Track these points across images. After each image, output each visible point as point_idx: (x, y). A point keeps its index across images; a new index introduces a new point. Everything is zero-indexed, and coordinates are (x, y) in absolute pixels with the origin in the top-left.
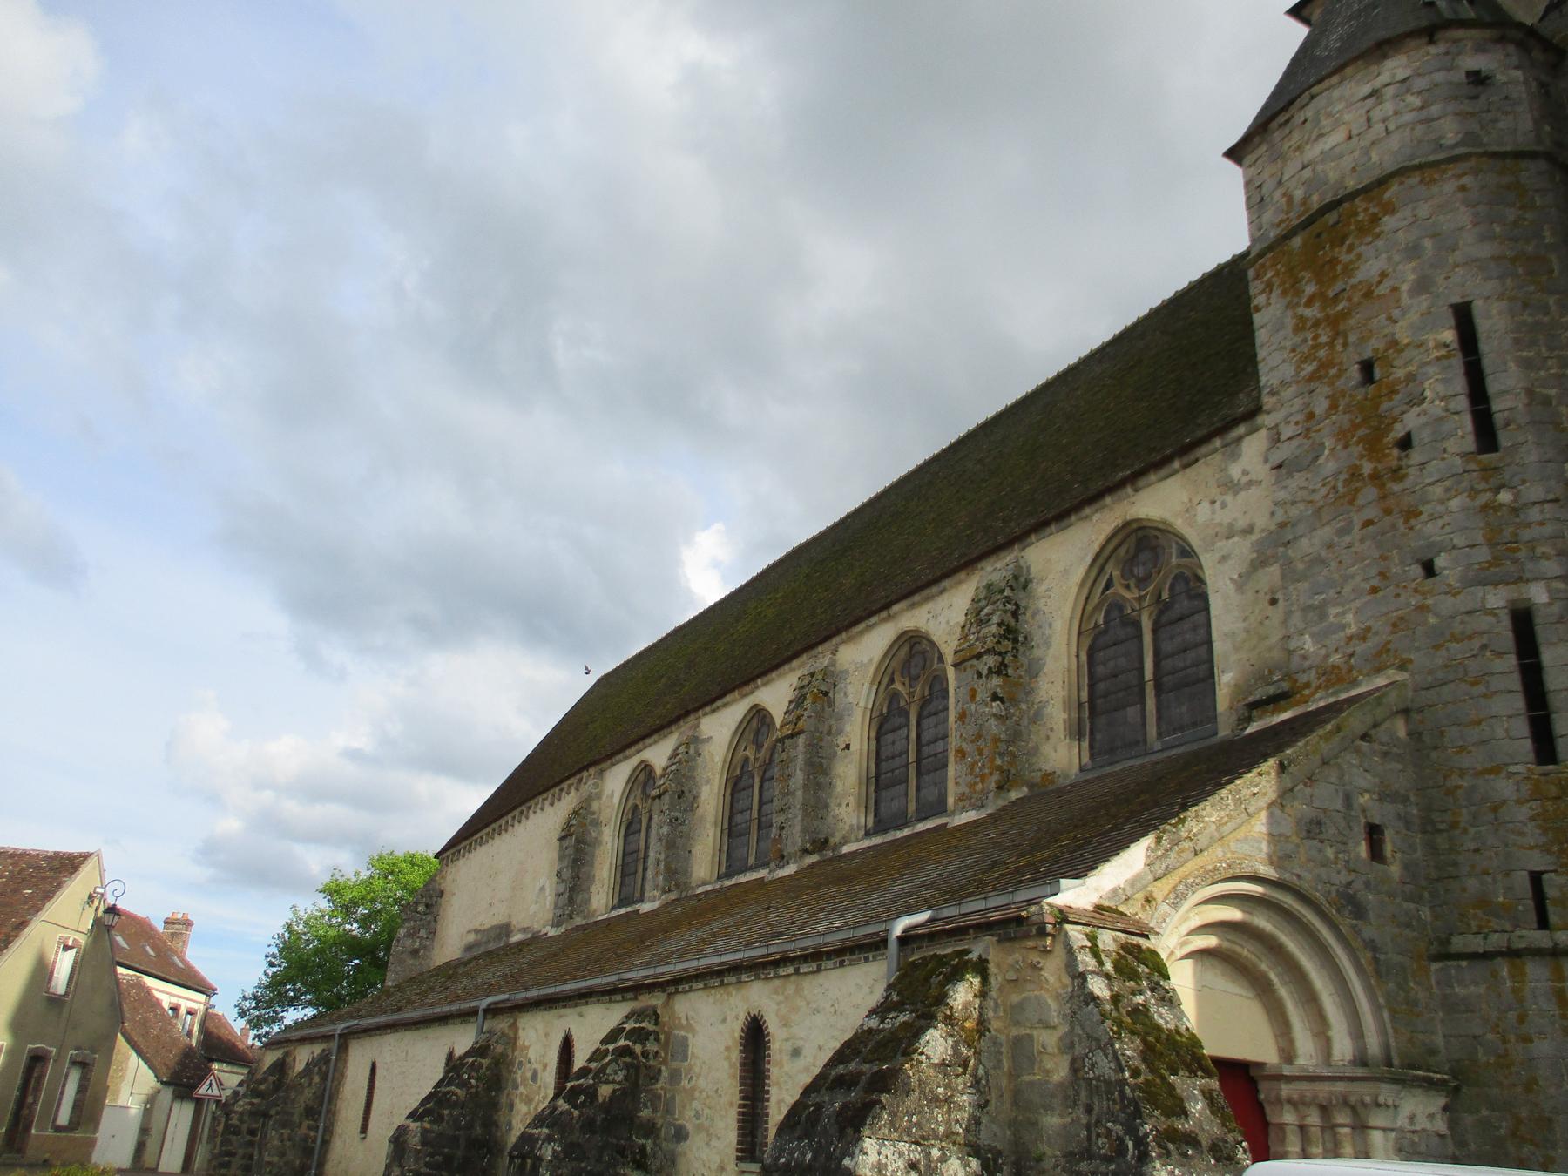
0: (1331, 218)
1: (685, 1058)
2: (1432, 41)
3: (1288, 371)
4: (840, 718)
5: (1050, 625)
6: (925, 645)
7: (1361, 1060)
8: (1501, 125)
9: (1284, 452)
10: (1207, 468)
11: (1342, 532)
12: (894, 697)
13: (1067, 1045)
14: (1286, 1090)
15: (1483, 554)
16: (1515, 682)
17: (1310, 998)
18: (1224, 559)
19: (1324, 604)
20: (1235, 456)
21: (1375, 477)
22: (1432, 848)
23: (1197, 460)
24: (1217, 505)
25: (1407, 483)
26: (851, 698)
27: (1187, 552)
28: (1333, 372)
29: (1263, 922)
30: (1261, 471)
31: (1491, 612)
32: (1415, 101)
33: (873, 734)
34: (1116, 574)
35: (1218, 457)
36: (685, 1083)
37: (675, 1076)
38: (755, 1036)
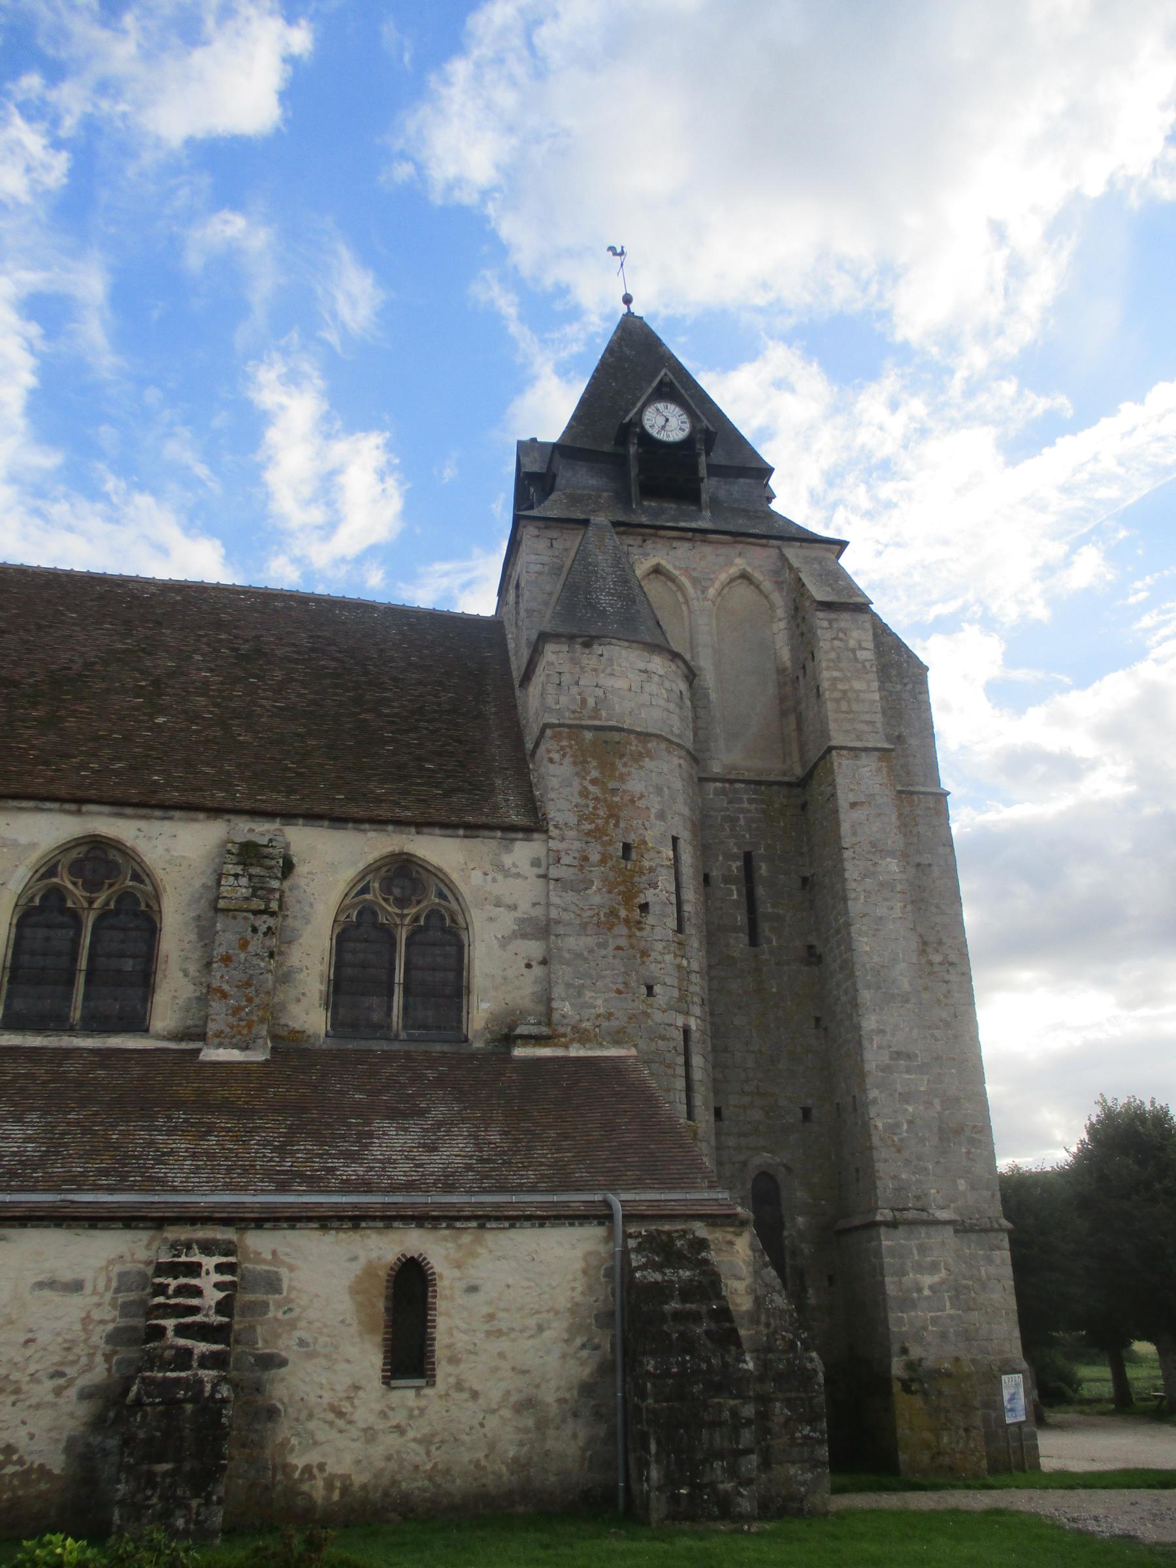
0: (616, 736)
1: (278, 1291)
3: (573, 820)
5: (311, 905)
11: (599, 945)
13: (751, 1290)
20: (509, 850)
21: (627, 921)
23: (477, 837)
24: (489, 878)
25: (644, 933)
28: (605, 838)
31: (677, 1027)
33: (15, 921)
35: (493, 844)
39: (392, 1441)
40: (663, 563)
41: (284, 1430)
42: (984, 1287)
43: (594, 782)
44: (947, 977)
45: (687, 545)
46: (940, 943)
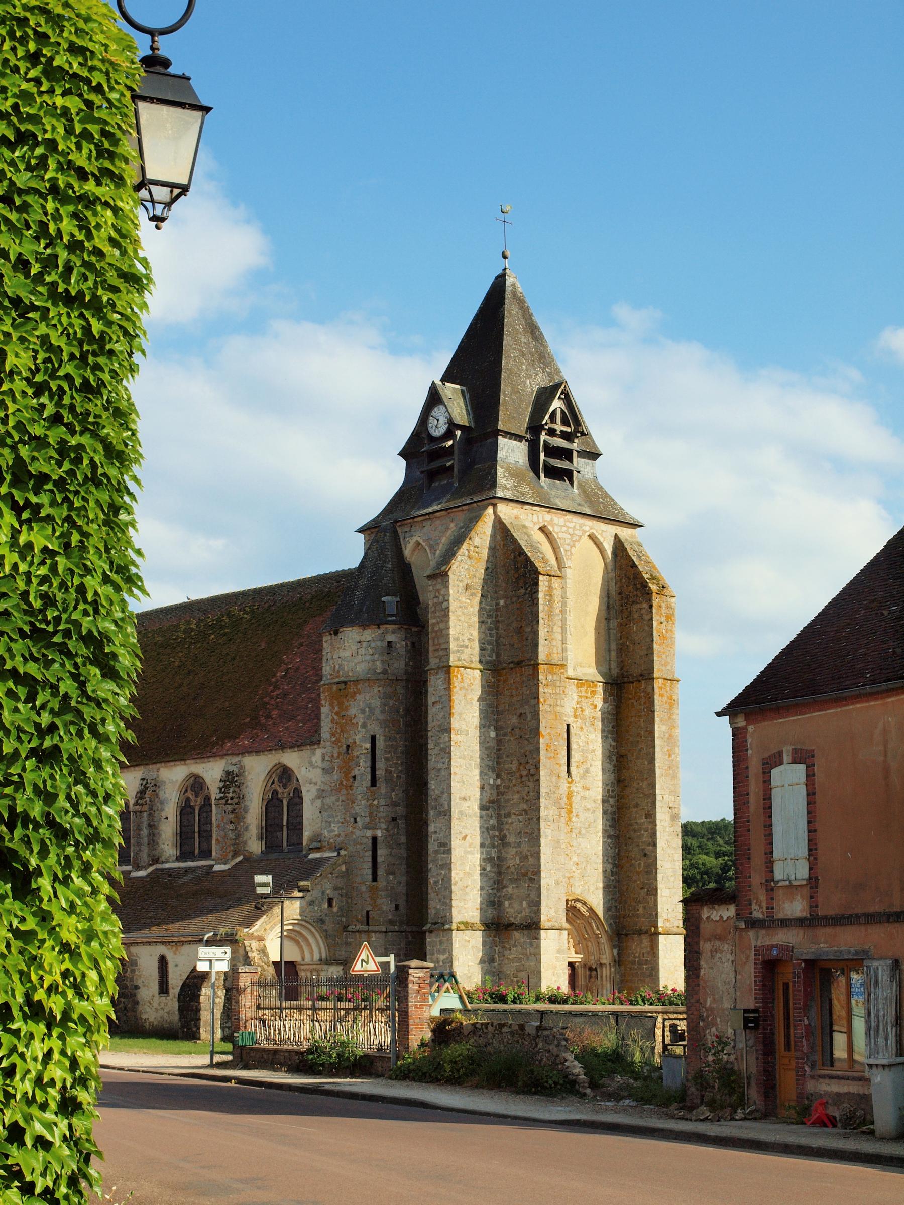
2: (379, 627)
4: (162, 803)
6: (201, 780)
7: (321, 960)
8: (395, 665)
9: (326, 765)
10: (306, 752)
11: (337, 800)
12: (188, 800)
14: (303, 967)
15: (367, 820)
16: (370, 859)
17: (309, 945)
18: (308, 791)
19: (330, 823)
20: (314, 754)
21: (346, 786)
22: (347, 902)
26: (167, 795)
27: (297, 780)
29: (297, 928)
30: (320, 763)
32: (371, 651)
34: (276, 780)
36: (137, 973)
37: (133, 971)
38: (163, 961)
39: (161, 1013)
40: (419, 539)
41: (140, 1008)
42: (528, 959)
43: (337, 714)
44: (529, 784)
45: (429, 523)
46: (528, 763)
